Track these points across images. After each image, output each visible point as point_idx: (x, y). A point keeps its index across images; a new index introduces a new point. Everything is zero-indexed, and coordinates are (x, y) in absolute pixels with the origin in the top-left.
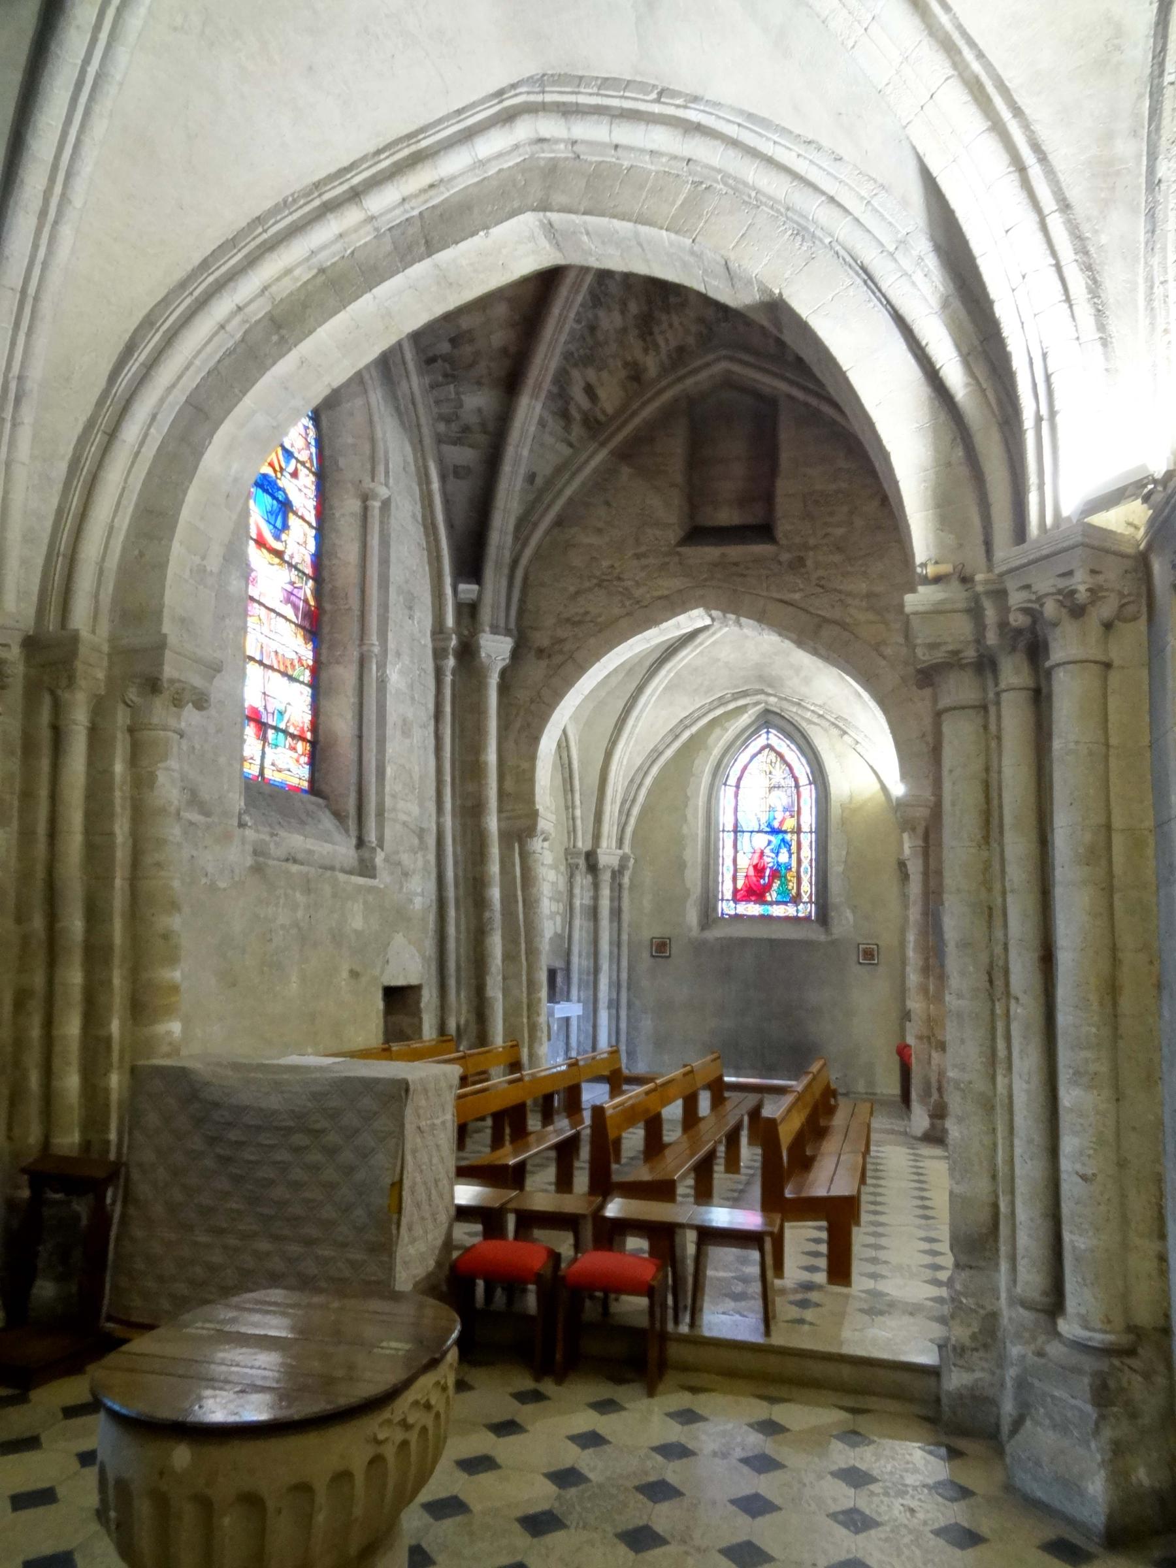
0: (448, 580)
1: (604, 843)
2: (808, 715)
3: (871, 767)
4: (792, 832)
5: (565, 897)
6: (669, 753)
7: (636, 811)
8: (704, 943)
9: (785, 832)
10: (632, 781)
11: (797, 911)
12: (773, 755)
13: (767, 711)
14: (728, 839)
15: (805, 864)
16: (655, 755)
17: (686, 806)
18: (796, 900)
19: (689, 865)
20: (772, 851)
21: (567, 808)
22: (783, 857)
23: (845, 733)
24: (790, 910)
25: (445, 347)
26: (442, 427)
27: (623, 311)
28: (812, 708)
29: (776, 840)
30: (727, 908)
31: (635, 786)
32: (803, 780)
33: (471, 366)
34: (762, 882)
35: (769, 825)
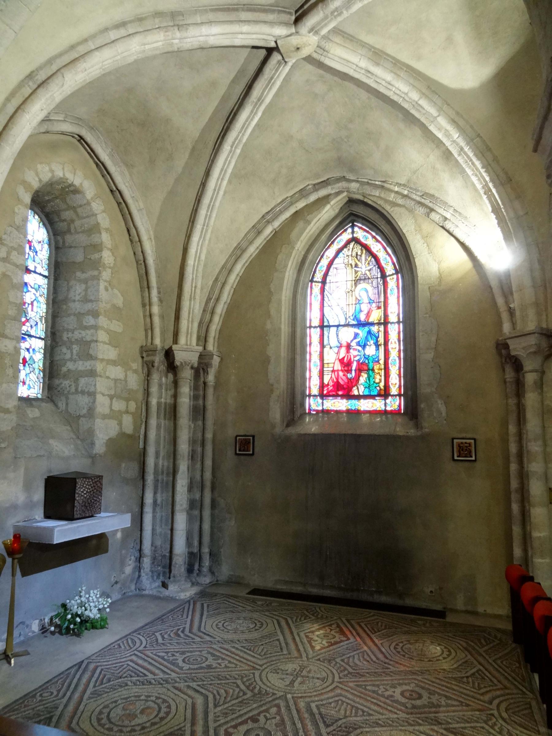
1: (182, 340)
2: (392, 197)
3: (462, 244)
4: (379, 324)
5: (140, 396)
6: (252, 250)
7: (220, 309)
8: (287, 439)
9: (372, 324)
10: (216, 280)
11: (385, 404)
12: (358, 249)
13: (351, 201)
14: (315, 334)
15: (394, 354)
16: (239, 253)
17: (269, 301)
18: (385, 394)
19: (272, 360)
20: (358, 344)
21: (144, 305)
22: (371, 350)
23: (432, 210)
24: (378, 404)
28: (396, 189)
29: (362, 332)
30: (314, 404)
31: (219, 284)
32: (389, 269)
34: (349, 376)
35: (355, 318)
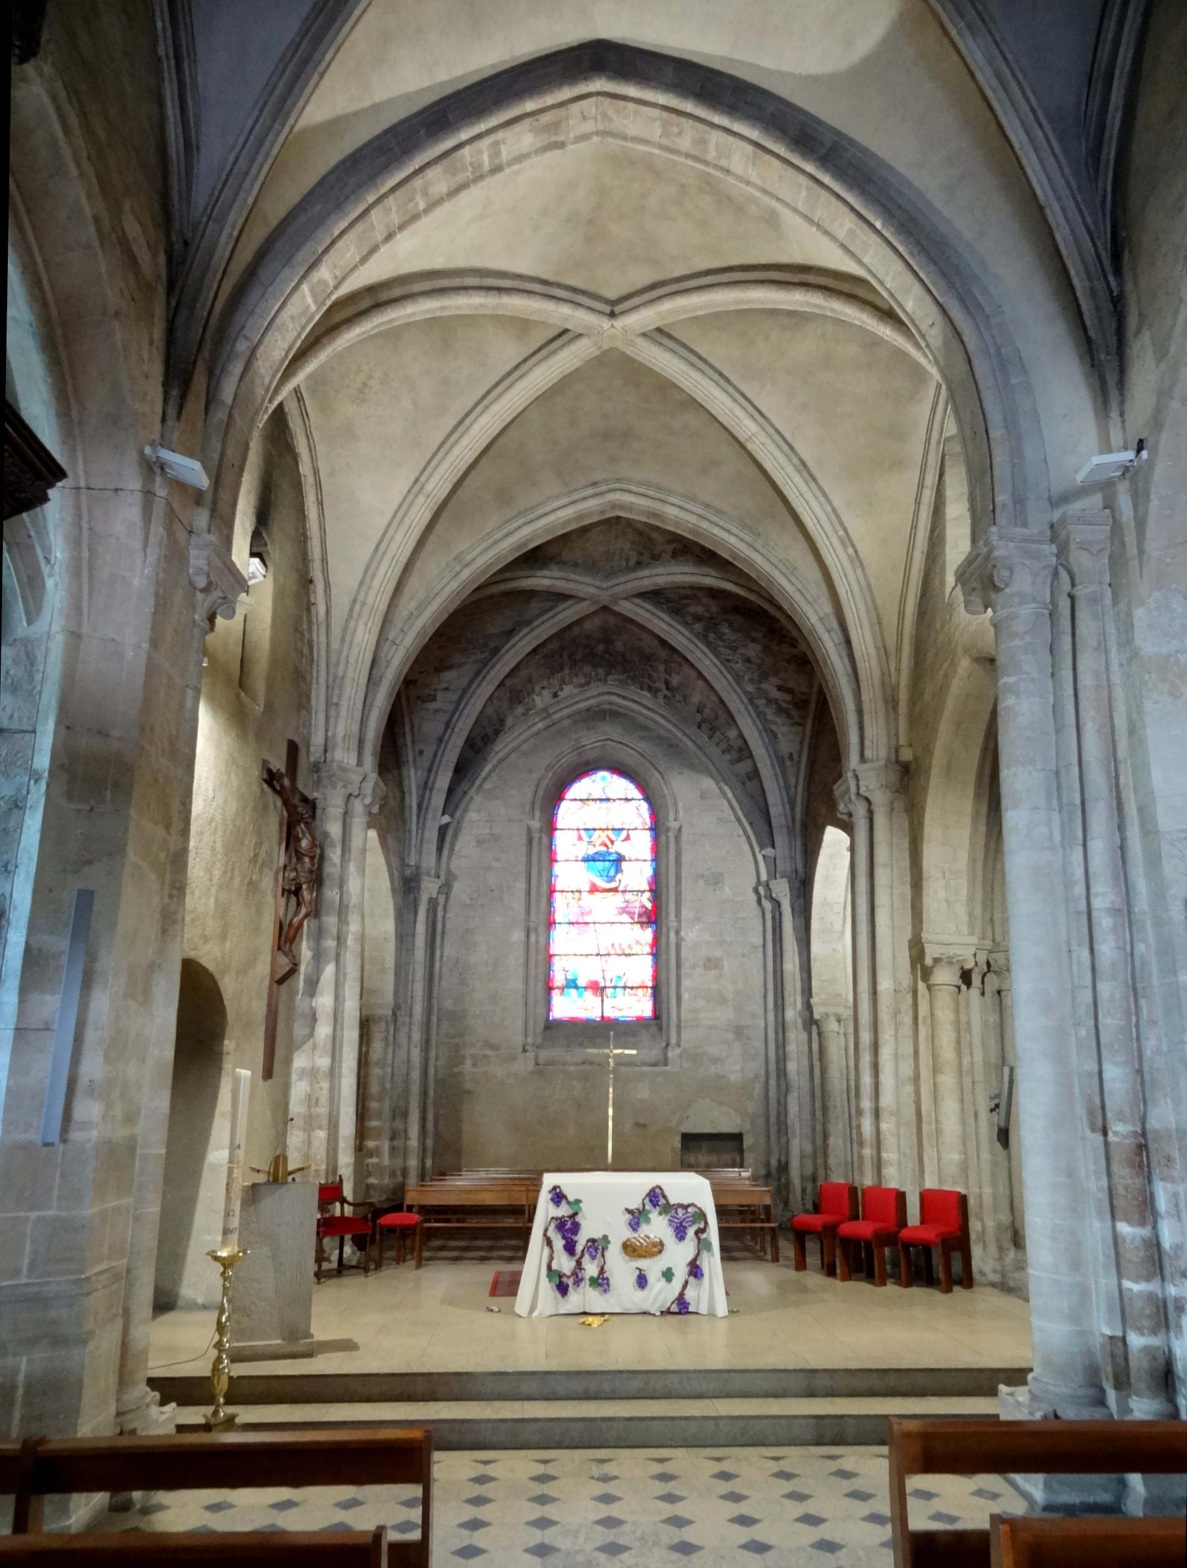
0: (757, 849)
25: (699, 717)
26: (727, 757)
27: (754, 640)
33: (717, 717)
